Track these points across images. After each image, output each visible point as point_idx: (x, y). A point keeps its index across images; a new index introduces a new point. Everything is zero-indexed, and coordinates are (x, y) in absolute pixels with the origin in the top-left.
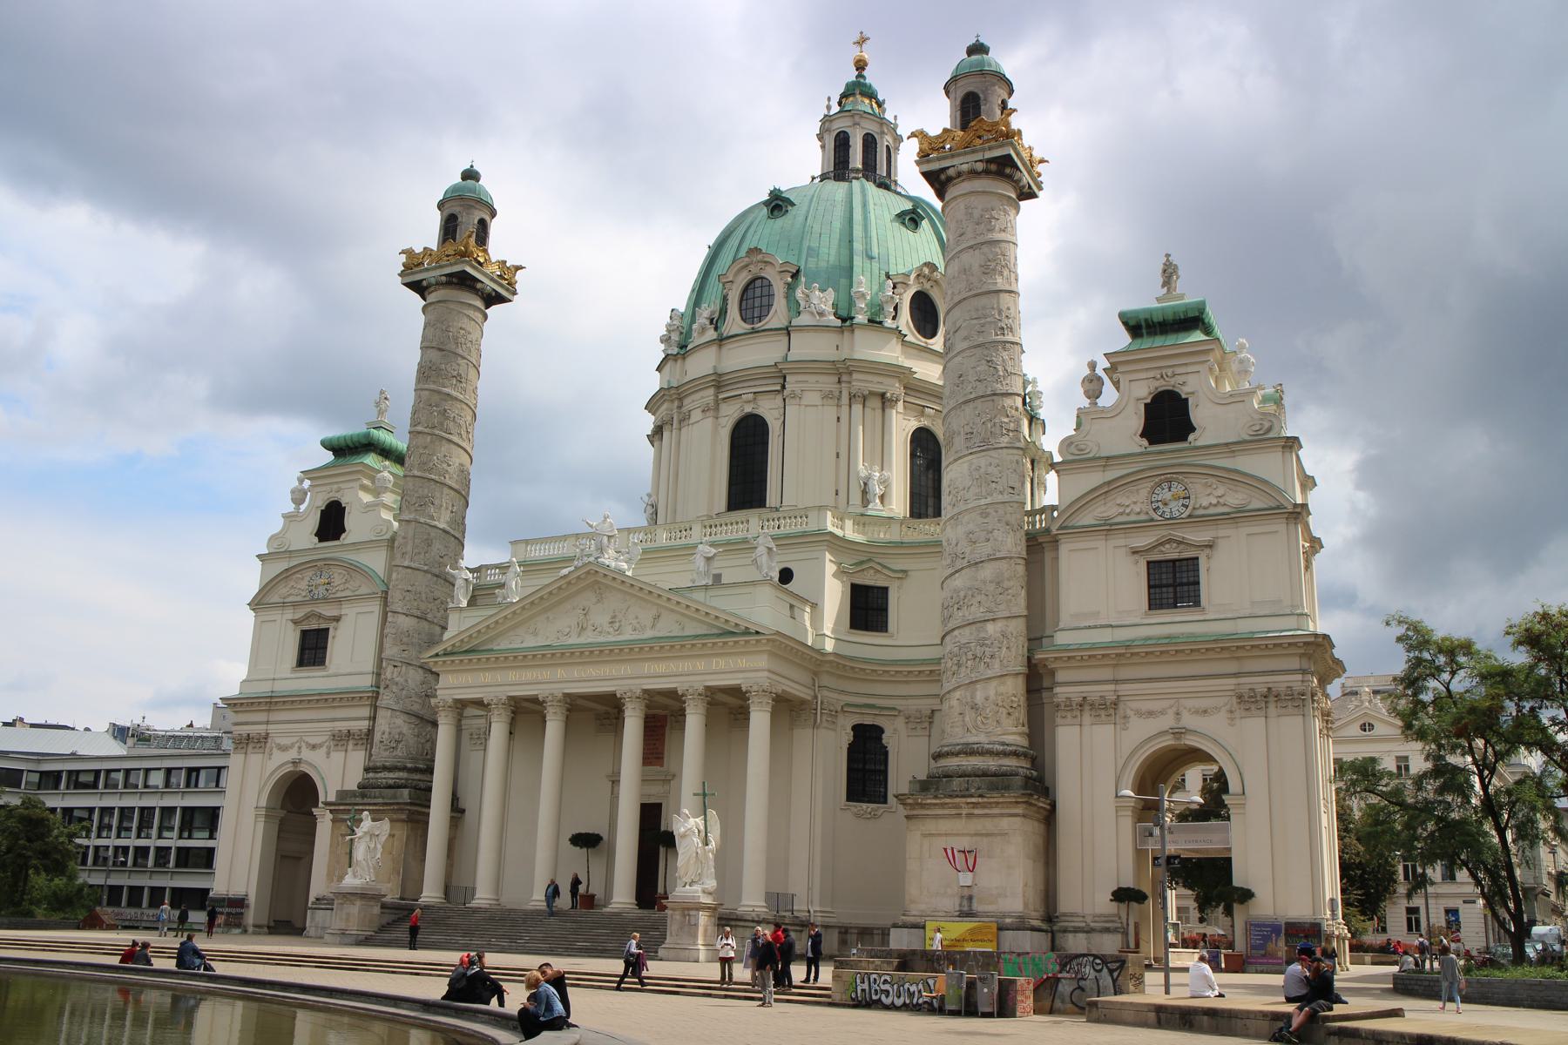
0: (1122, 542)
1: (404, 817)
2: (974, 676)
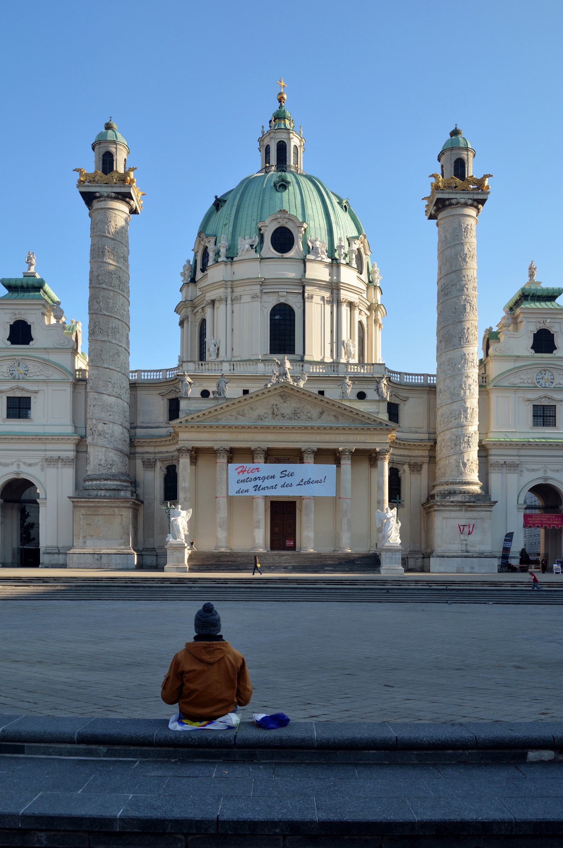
0: (521, 395)
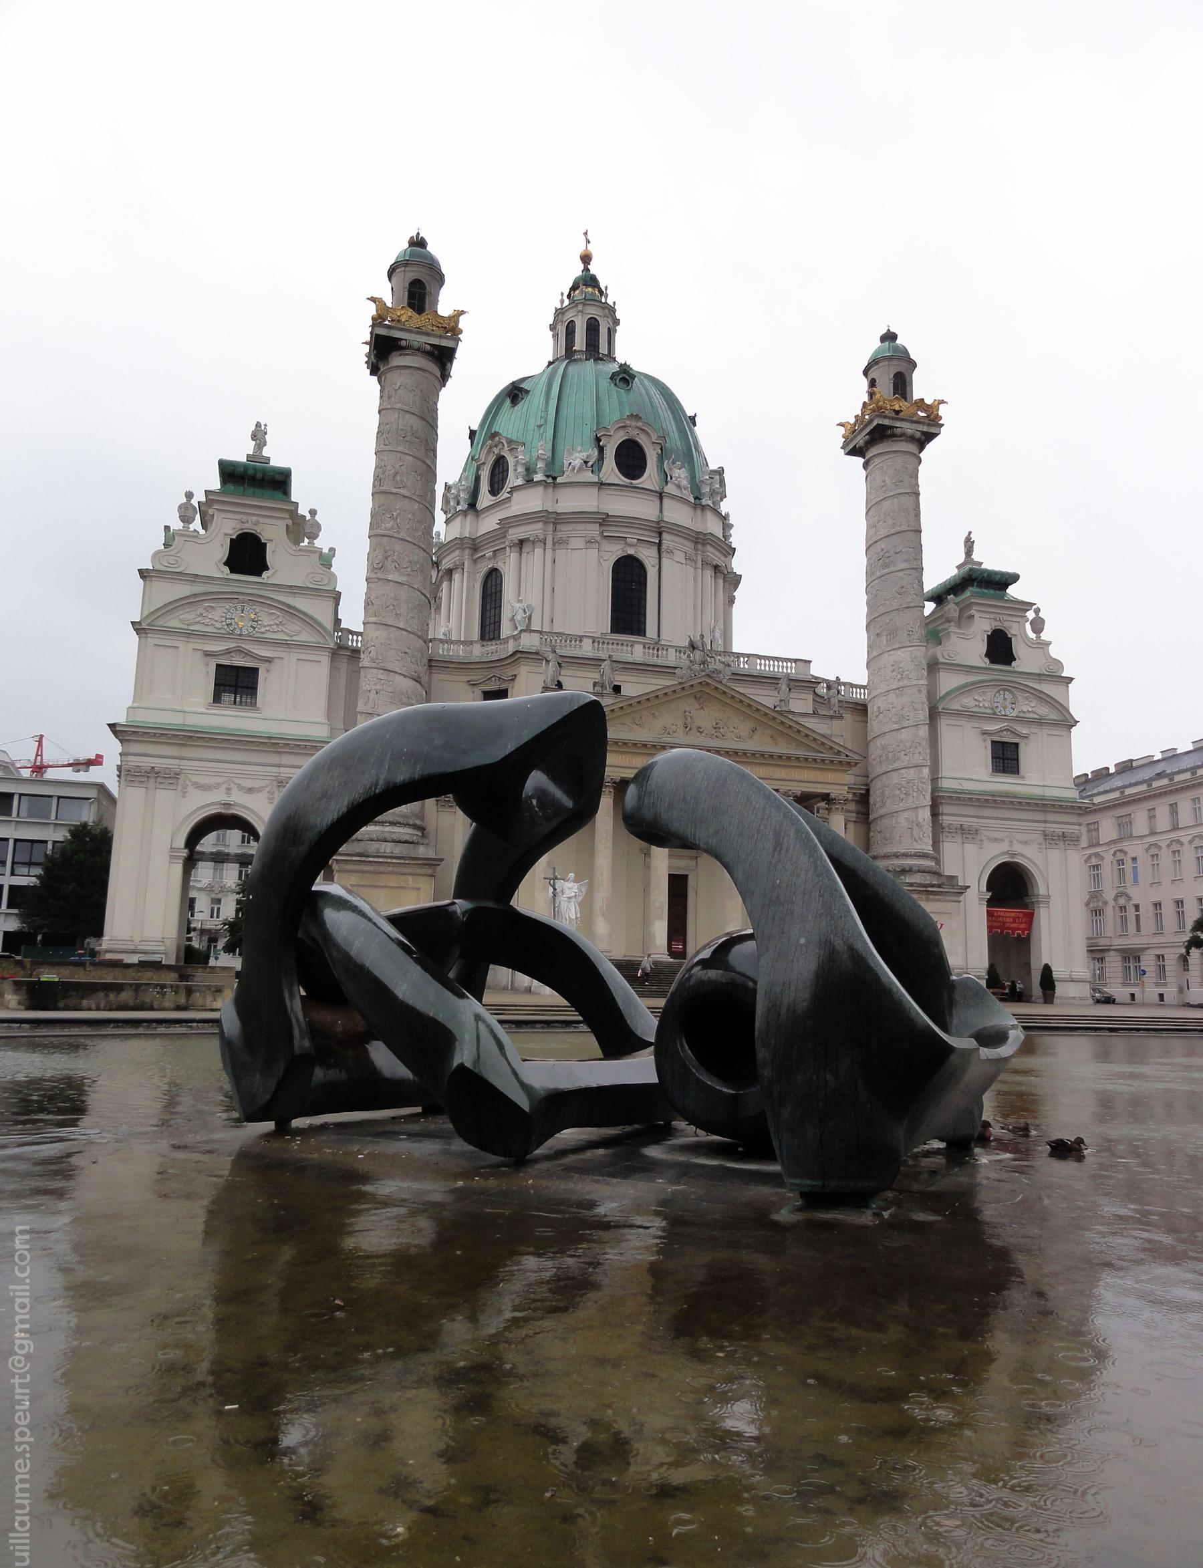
2: (918, 803)
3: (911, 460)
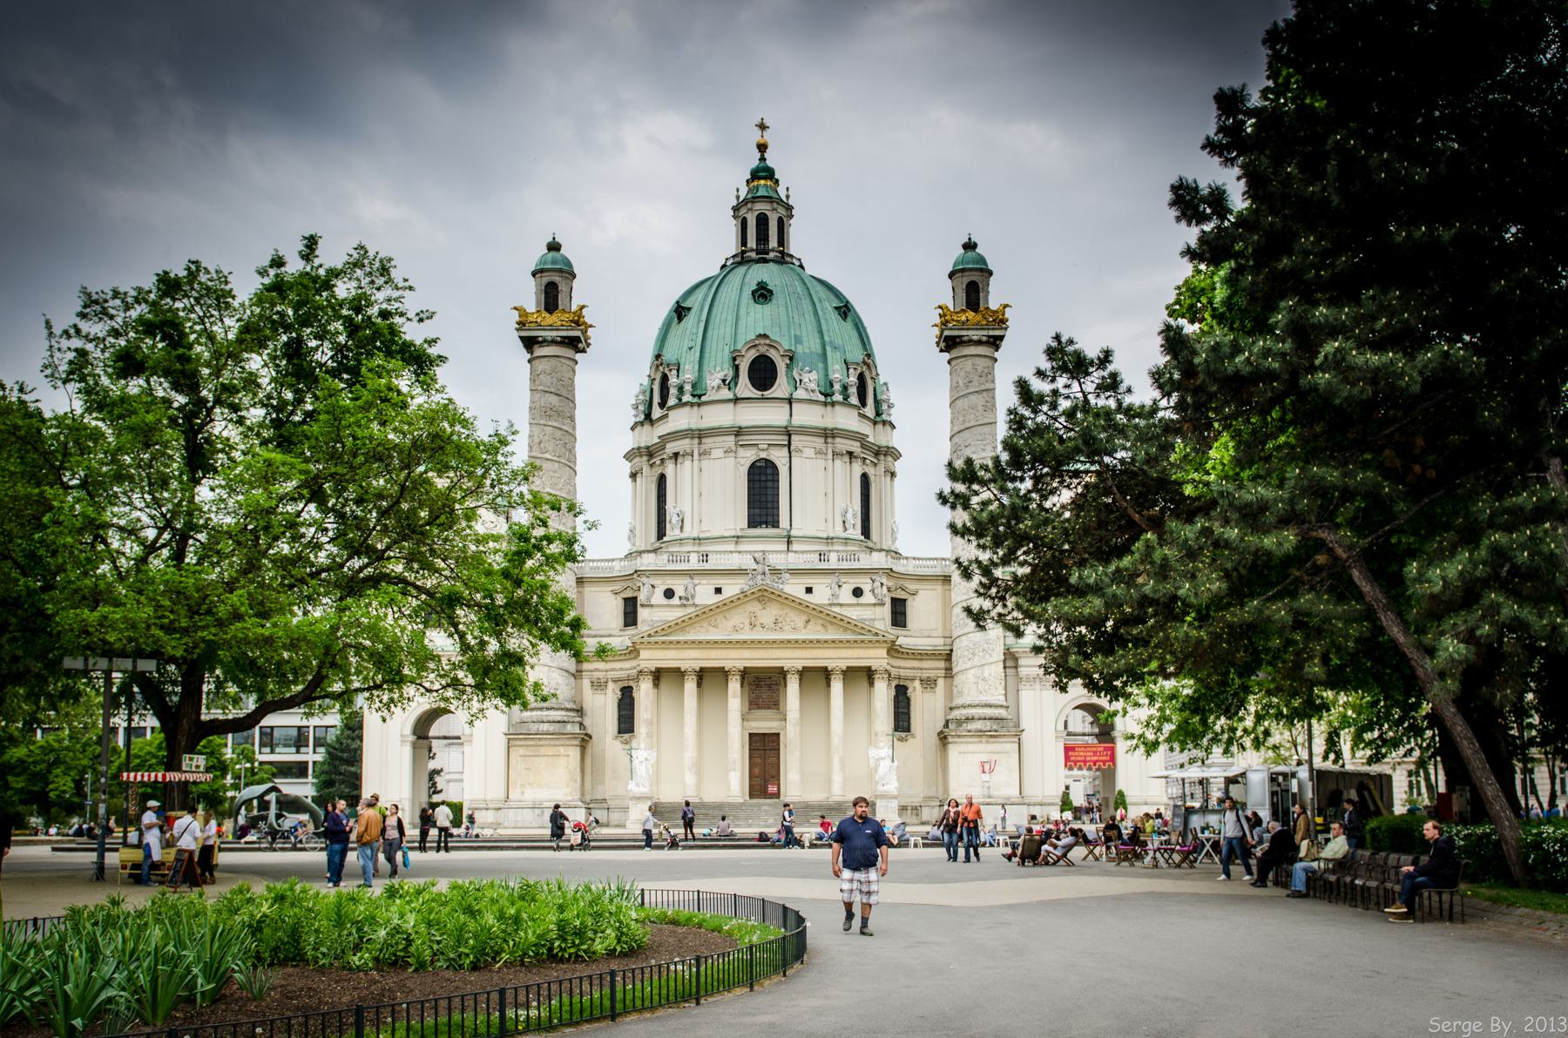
1: (576, 742)
2: (983, 662)
3: (982, 363)
